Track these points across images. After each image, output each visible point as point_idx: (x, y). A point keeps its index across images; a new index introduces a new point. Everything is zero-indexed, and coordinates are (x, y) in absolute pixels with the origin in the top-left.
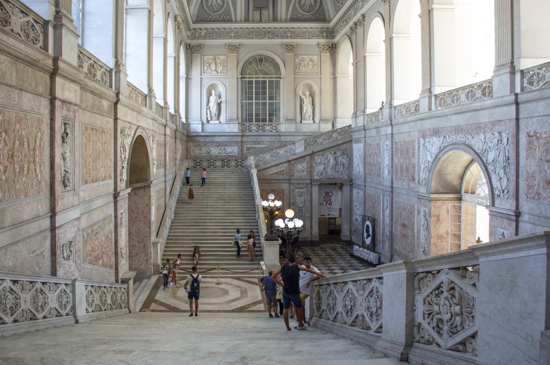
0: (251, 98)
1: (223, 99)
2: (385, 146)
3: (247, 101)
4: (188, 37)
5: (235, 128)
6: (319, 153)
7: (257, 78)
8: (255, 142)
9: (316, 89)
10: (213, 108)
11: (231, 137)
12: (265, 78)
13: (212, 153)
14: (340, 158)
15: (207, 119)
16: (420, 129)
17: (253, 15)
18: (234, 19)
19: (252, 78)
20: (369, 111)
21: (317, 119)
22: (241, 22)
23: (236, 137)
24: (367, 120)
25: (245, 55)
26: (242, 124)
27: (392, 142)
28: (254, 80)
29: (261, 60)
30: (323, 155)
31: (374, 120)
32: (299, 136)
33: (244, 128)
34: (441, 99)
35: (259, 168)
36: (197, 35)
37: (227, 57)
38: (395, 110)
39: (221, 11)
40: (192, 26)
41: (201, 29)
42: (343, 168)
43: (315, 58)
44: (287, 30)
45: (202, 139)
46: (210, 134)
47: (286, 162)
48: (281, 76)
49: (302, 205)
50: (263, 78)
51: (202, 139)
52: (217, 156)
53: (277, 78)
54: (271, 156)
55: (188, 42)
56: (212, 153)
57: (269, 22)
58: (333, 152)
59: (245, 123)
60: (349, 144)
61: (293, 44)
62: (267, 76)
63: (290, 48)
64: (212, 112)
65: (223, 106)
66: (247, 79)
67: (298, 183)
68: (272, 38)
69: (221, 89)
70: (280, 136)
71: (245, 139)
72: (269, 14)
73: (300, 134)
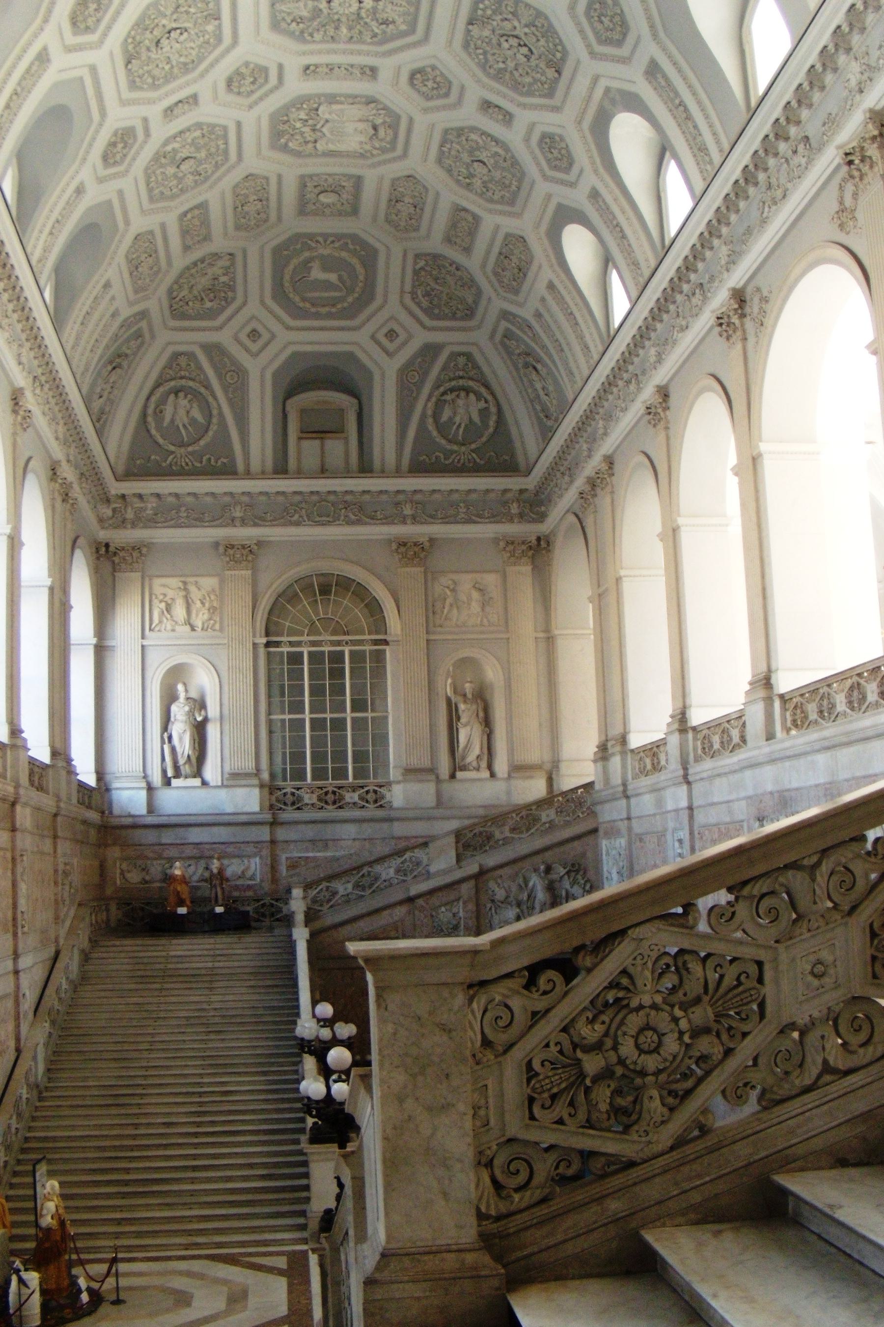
0: (297, 707)
1: (213, 710)
2: (677, 844)
3: (287, 717)
4: (101, 520)
5: (248, 800)
7: (314, 644)
8: (313, 841)
9: (492, 673)
10: (181, 739)
11: (238, 829)
12: (339, 643)
14: (566, 884)
15: (164, 772)
16: (750, 792)
17: (299, 453)
18: (240, 467)
20: (636, 741)
21: (501, 765)
22: (263, 475)
23: (253, 828)
24: (633, 768)
25: (275, 578)
26: (270, 788)
27: (691, 833)
28: (305, 651)
29: (327, 587)
30: (513, 878)
31: (649, 767)
32: (448, 818)
33: (278, 800)
34: (795, 707)
35: (318, 925)
36: (130, 515)
38: (695, 739)
39: (202, 443)
40: (116, 488)
41: (140, 496)
44: (401, 497)
45: (150, 837)
46: (174, 820)
47: (401, 903)
48: (388, 639)
52: (197, 888)
54: (357, 886)
55: (103, 535)
57: (347, 473)
58: (542, 867)
59: (281, 783)
60: (589, 840)
61: (421, 540)
63: (413, 552)
64: (179, 750)
65: (213, 732)
66: (285, 649)
68: (359, 522)
69: (204, 679)
70: (390, 820)
71: (282, 834)
73: (448, 813)
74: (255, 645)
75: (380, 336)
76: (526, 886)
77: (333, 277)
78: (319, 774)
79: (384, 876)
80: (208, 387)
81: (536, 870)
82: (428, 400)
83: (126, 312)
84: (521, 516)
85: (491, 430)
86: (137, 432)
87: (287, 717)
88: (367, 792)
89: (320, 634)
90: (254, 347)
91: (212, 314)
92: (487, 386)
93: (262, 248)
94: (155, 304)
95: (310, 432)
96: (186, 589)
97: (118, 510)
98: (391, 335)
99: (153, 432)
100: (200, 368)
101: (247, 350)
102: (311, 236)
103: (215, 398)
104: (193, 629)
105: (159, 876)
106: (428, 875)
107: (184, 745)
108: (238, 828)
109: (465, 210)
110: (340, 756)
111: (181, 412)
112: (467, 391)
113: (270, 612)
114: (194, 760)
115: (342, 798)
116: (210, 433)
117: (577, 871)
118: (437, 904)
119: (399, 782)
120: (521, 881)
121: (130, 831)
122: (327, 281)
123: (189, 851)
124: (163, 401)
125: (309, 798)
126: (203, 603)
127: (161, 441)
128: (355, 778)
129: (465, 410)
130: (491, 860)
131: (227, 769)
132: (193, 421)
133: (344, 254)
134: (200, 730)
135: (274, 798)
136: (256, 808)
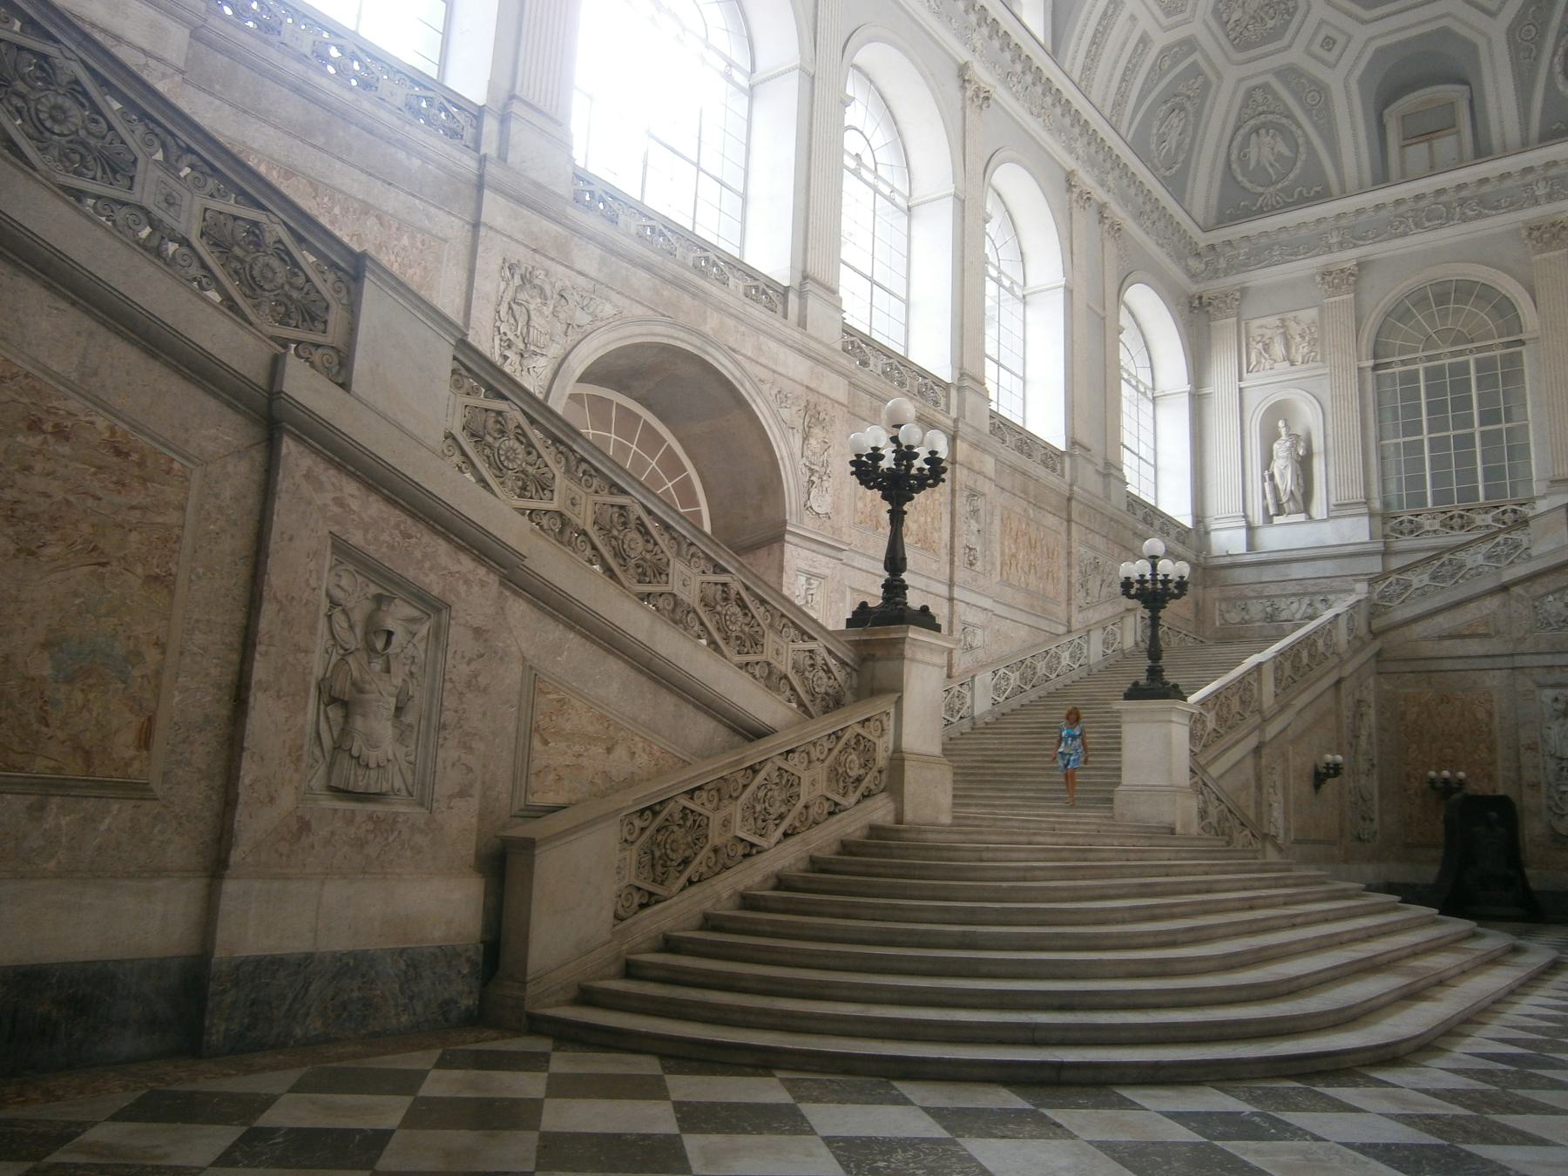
1: (1318, 444)
3: (1401, 440)
4: (1193, 276)
5: (1356, 531)
7: (1429, 359)
10: (1282, 476)
12: (1461, 353)
15: (1266, 509)
17: (1403, 162)
18: (1335, 187)
19: (1413, 361)
22: (1361, 190)
23: (1363, 559)
25: (1381, 294)
28: (1421, 367)
29: (1446, 295)
37: (1322, 310)
39: (1291, 176)
40: (1202, 240)
45: (1250, 575)
47: (1491, 593)
48: (1522, 337)
50: (1453, 354)
51: (1250, 575)
54: (1433, 578)
55: (1195, 289)
56: (1284, 615)
57: (1460, 163)
62: (1470, 346)
64: (1281, 487)
65: (1318, 465)
68: (1479, 216)
69: (1309, 416)
72: (1460, 143)
79: (1469, 564)
80: (1290, 116)
82: (1554, 54)
83: (1160, 40)
87: (1401, 440)
88: (1504, 513)
89: (1438, 347)
90: (1331, 57)
91: (1276, 34)
95: (1412, 137)
96: (1283, 326)
97: (1209, 260)
99: (1240, 178)
100: (1277, 97)
101: (1323, 61)
103: (1299, 126)
105: (1262, 615)
108: (1347, 561)
110: (1468, 475)
111: (1266, 149)
113: (1378, 334)
114: (1299, 498)
116: (1299, 164)
118: (1541, 591)
119: (1544, 497)
121: (1228, 572)
123: (1292, 588)
125: (1428, 524)
126: (1302, 337)
127: (1248, 185)
131: (1333, 501)
132: (1279, 157)
134: (1304, 465)
135: (1388, 528)
136: (1367, 539)
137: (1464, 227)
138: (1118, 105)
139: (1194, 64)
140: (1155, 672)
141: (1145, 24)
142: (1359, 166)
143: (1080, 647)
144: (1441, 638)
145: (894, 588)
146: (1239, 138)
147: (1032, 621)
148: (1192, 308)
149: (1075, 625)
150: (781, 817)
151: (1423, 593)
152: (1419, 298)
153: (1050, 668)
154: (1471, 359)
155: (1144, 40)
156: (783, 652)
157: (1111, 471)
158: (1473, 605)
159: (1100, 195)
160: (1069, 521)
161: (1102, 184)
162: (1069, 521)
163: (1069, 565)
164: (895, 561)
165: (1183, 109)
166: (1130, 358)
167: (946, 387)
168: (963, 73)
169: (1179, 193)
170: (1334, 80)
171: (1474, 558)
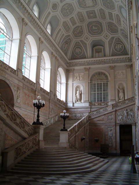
1: (83, 92)
4: (67, 66)
6: (119, 110)
7: (97, 82)
9: (125, 85)
12: (101, 82)
13: (77, 116)
14: (130, 112)
15: (75, 101)
17: (95, 55)
22: (90, 58)
25: (92, 73)
29: (100, 74)
36: (71, 65)
37: (84, 74)
40: (69, 61)
41: (72, 62)
42: (131, 117)
43: (124, 71)
45: (73, 110)
47: (103, 115)
49: (111, 136)
53: (107, 81)
54: (97, 113)
55: (67, 68)
56: (77, 116)
58: (126, 110)
60: (134, 105)
65: (83, 95)
67: (109, 125)
68: (104, 64)
69: (82, 88)
74: (89, 82)
75: (105, 36)
76: (123, 112)
77: (96, 28)
78: (98, 101)
80: (81, 47)
81: (125, 110)
83: (65, 35)
84: (129, 61)
85: (123, 49)
86: (72, 54)
91: (81, 36)
92: (122, 42)
93: (85, 25)
94: (71, 33)
98: (107, 36)
102: (92, 22)
103: (82, 48)
104: (80, 80)
106: (108, 111)
107: (78, 97)
109: (110, 12)
110: (101, 98)
111: (78, 50)
112: (119, 43)
114: (80, 99)
115: (101, 104)
117: (132, 110)
120: (122, 112)
122: (96, 29)
124: (75, 49)
125: (96, 104)
128: (103, 101)
129: (119, 47)
130: (117, 109)
133: (97, 24)
136: (88, 106)
137: (102, 65)
138: (59, 43)
139: (69, 38)
140: (64, 128)
141: (64, 33)
142: (90, 55)
143: (50, 121)
144: (97, 121)
145: (38, 120)
146: (74, 49)
147: (44, 117)
148: (67, 71)
149: (50, 117)
150: (28, 148)
151: (95, 115)
152: (96, 74)
153: (46, 124)
154: (102, 83)
155: (63, 35)
156: (27, 128)
157: (55, 95)
158: (101, 117)
159: (56, 55)
160: (50, 102)
161: (56, 54)
162: (50, 102)
163: (49, 109)
164: (38, 116)
165: (67, 44)
166: (58, 79)
167: (35, 83)
168: (40, 39)
169: (66, 54)
170: (87, 43)
171: (101, 110)
